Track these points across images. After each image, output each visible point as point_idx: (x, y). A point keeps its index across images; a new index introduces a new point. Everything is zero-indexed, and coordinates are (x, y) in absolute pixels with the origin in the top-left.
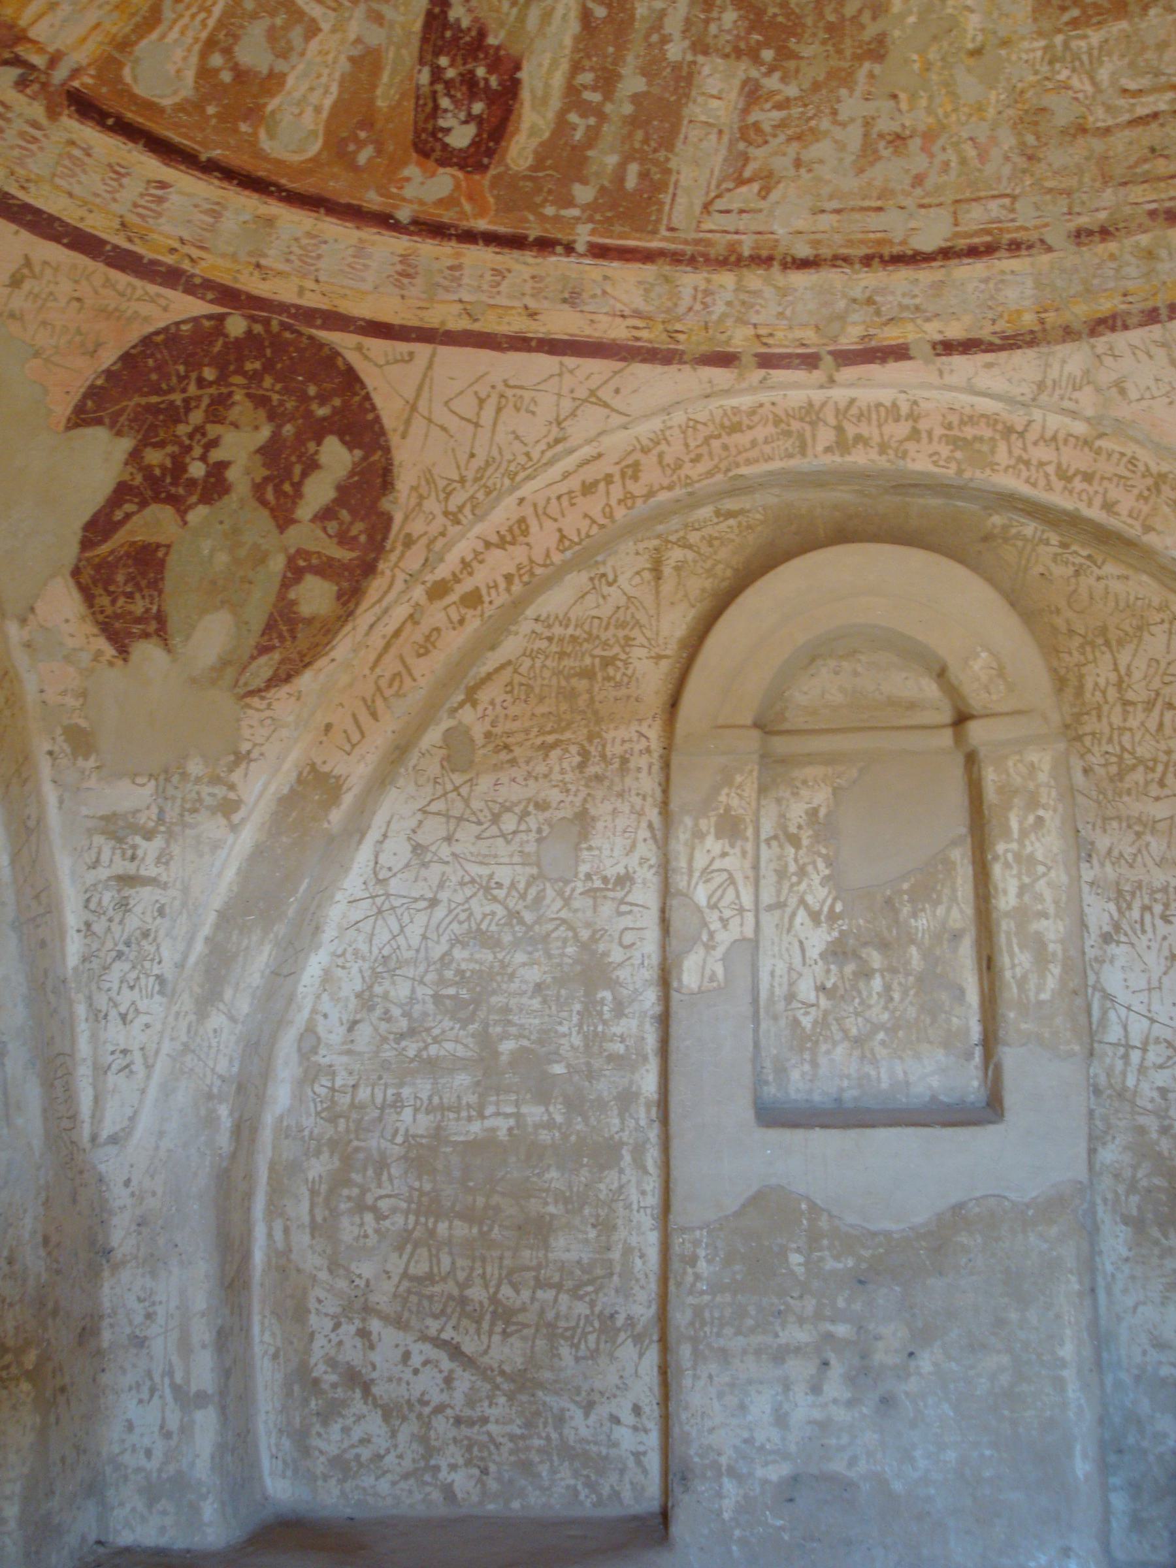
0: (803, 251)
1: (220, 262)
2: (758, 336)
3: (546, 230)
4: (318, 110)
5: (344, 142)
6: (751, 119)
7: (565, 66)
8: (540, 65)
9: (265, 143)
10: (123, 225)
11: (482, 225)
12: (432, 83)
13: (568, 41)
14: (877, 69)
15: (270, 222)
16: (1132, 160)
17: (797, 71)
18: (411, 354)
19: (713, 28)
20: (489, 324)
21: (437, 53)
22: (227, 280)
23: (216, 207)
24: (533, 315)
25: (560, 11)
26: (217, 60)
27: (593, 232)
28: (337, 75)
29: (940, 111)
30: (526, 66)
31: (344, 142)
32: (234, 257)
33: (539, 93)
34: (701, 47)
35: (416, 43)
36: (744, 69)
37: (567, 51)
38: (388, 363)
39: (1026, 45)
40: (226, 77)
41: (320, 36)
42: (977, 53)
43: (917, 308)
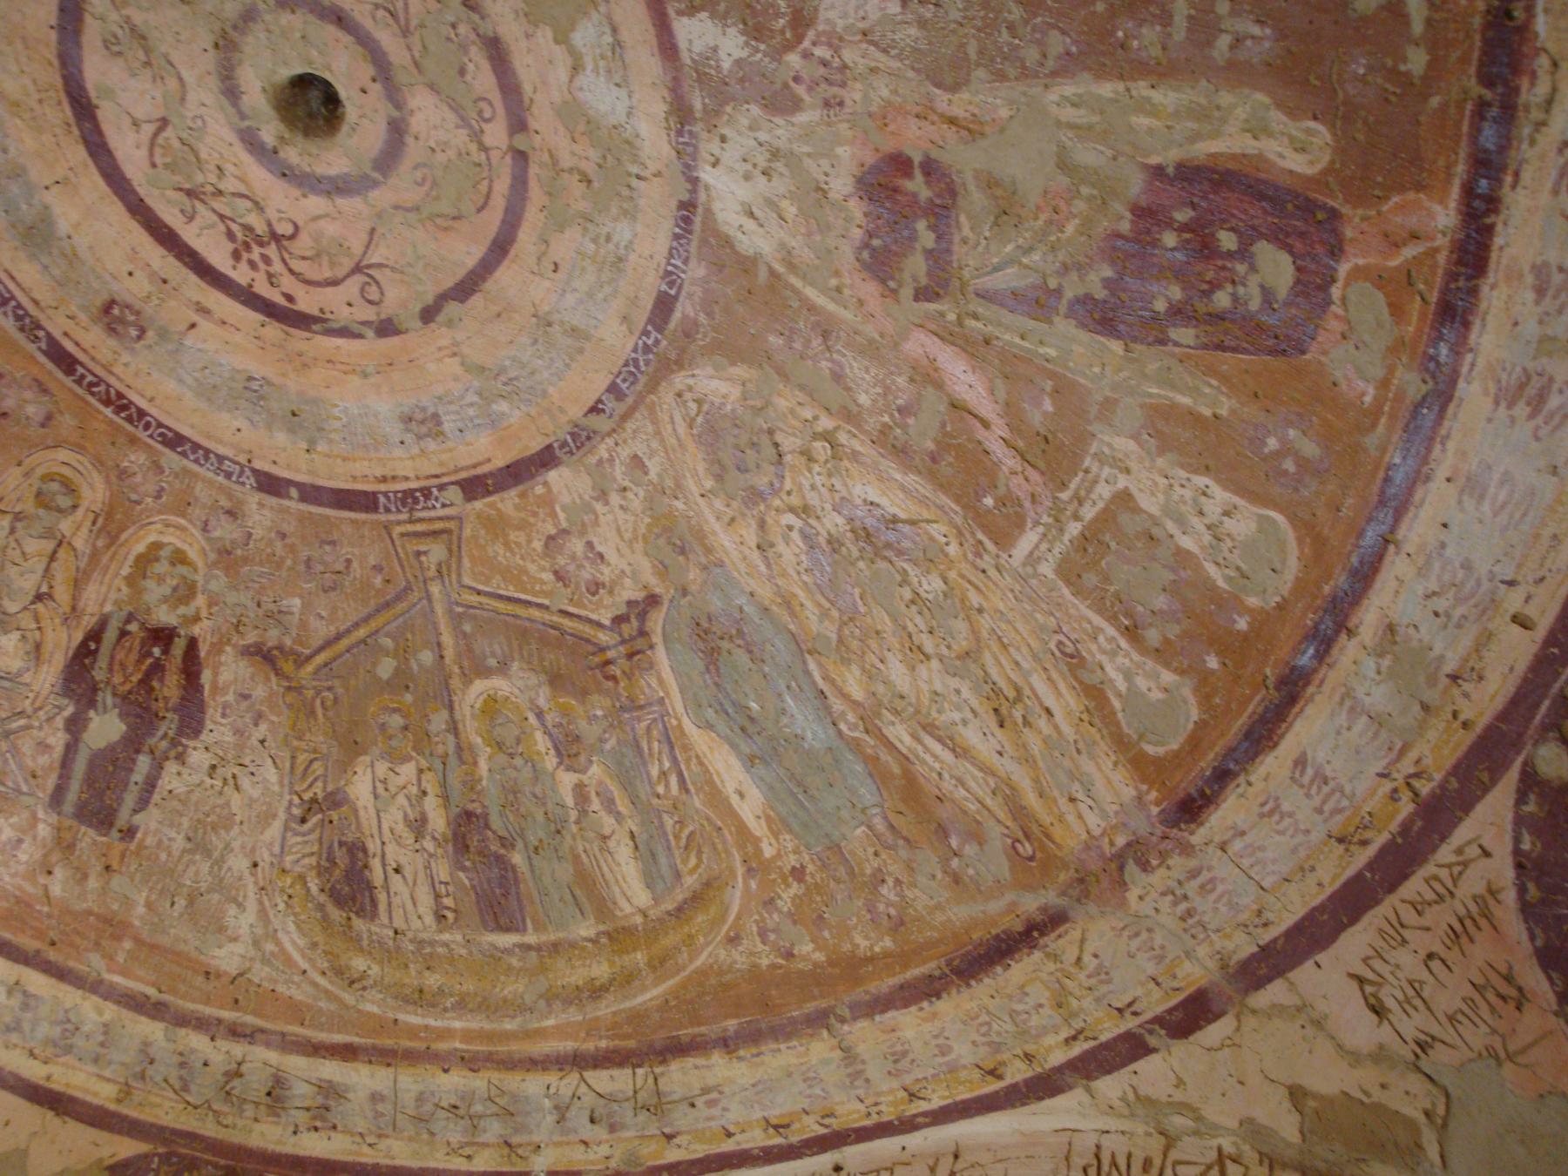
1: (1431, 735)
3: (1464, 60)
7: (1141, 88)
8: (1151, 131)
10: (1341, 840)
13: (1107, 89)
23: (1348, 703)
25: (1069, 114)
28: (1183, 474)
30: (1154, 160)
37: (1121, 86)
41: (1134, 491)
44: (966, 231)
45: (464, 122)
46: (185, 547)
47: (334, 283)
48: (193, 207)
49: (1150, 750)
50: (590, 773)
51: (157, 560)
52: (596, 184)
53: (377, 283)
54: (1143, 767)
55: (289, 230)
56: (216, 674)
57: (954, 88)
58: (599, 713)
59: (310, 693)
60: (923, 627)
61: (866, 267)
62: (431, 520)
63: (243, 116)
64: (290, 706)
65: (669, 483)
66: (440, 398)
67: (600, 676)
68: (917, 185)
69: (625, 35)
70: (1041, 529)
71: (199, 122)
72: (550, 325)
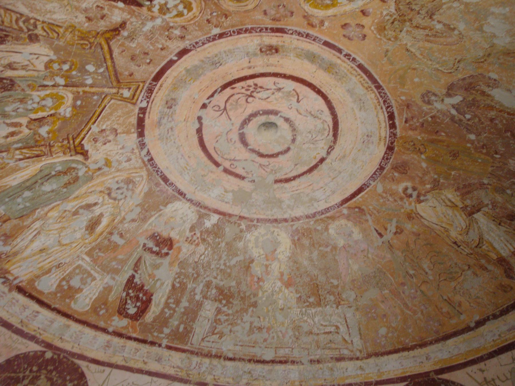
0: (231, 355)
2: (215, 379)
4: (91, 299)
5: (97, 308)
6: (218, 317)
7: (166, 297)
8: (159, 296)
9: (72, 305)
11: (134, 335)
12: (126, 296)
13: (167, 291)
14: (254, 310)
15: (68, 326)
16: (325, 343)
17: (232, 307)
18: (104, 371)
19: (209, 293)
20: (131, 364)
21: (129, 289)
22: (49, 341)
24: (145, 363)
25: (166, 283)
26: (64, 283)
27: (167, 342)
28: (99, 291)
29: (272, 323)
31: (97, 308)
32: (54, 335)
33: (157, 303)
34: (205, 297)
35: (123, 286)
36: (217, 304)
37: (167, 293)
38: (95, 372)
39: (295, 309)
40: (66, 287)
42: (282, 309)
43: (264, 376)
44: (153, 258)
45: (234, 160)
46: (182, 18)
47: (226, 102)
48: (276, 86)
49: (36, 284)
50: (26, 128)
51: (185, 8)
52: (201, 177)
53: (218, 111)
54: (32, 281)
55: (249, 100)
56: (120, 9)
57: (179, 264)
58: (50, 135)
59: (92, 40)
60: (68, 233)
61: (154, 233)
62: (139, 95)
63: (281, 116)
64: (89, 32)
65: (120, 167)
66: (175, 111)
67: (64, 138)
68: (165, 250)
69: (224, 203)
70: (89, 261)
71: (290, 107)
72: (177, 148)
